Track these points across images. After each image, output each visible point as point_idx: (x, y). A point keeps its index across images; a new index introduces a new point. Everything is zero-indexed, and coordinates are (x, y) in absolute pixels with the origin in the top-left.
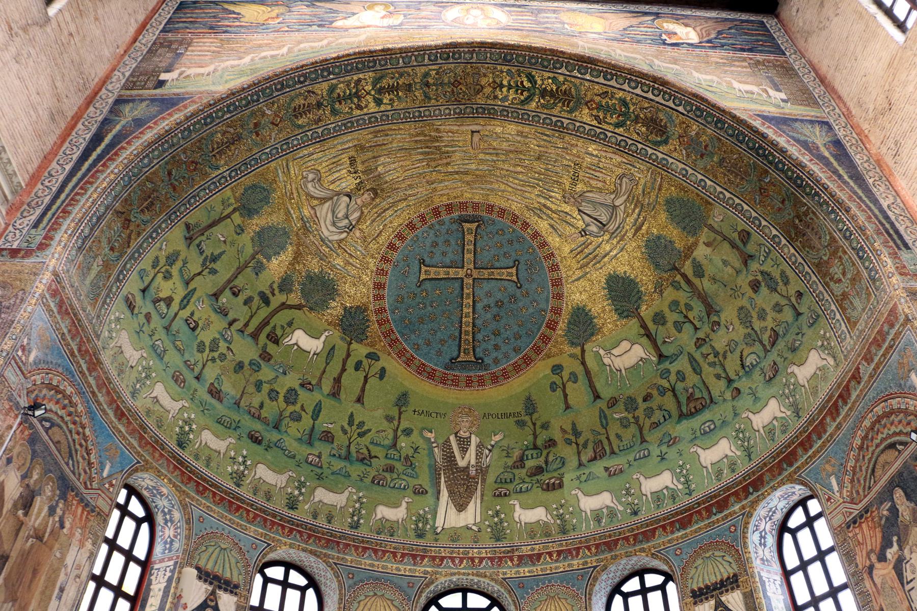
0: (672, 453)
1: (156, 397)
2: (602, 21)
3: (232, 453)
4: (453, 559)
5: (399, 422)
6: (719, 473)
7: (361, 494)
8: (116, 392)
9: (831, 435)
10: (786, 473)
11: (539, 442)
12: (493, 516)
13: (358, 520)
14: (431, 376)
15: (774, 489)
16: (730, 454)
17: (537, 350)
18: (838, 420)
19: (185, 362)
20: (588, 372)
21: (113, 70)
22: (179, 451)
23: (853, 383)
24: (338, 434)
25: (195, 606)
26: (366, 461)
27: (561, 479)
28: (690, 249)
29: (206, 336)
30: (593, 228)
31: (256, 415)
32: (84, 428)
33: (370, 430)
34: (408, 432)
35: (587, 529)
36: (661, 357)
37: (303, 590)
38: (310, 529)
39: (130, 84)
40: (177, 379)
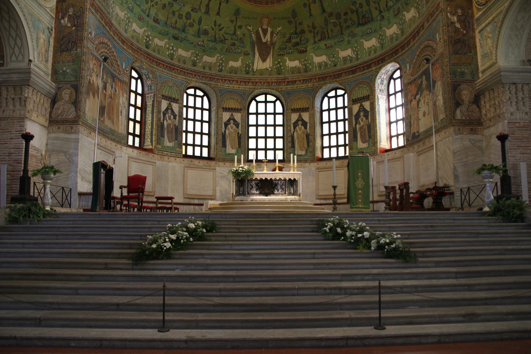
1: (134, 30)
3: (168, 46)
4: (261, 83)
5: (236, 23)
7: (222, 57)
8: (120, 33)
9: (411, 47)
10: (394, 58)
11: (298, 31)
12: (277, 64)
13: (222, 68)
15: (388, 63)
16: (375, 45)
18: (415, 41)
19: (142, 10)
22: (147, 50)
23: (421, 28)
24: (210, 30)
25: (164, 109)
26: (223, 42)
27: (306, 48)
31: (175, 27)
32: (113, 53)
33: (223, 28)
34: (240, 27)
35: (315, 71)
37: (202, 97)
38: (203, 74)
40: (140, 19)
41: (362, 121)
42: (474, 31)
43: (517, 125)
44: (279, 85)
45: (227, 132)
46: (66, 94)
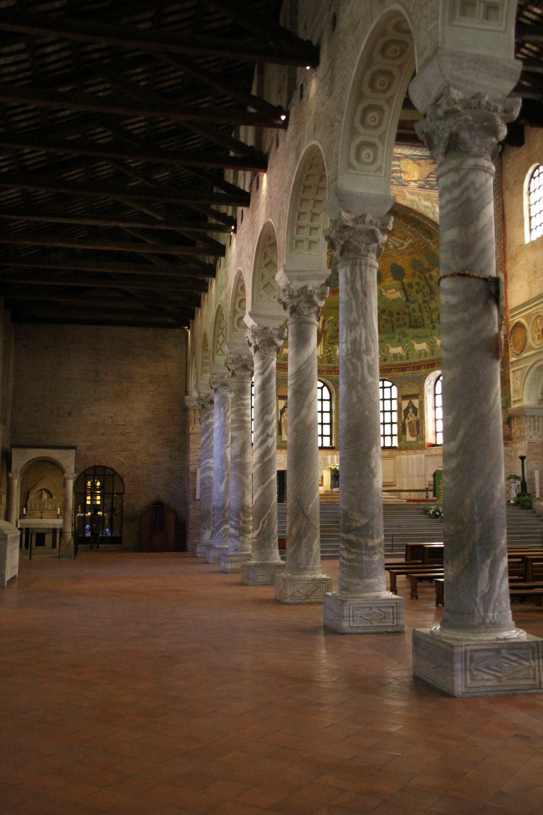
0: (404, 340)
2: (418, 168)
6: (420, 355)
12: (328, 352)
15: (438, 369)
16: (426, 349)
28: (429, 270)
30: (391, 247)
36: (407, 300)
41: (411, 416)
42: (509, 369)
43: (534, 444)
44: (330, 374)
45: (283, 420)
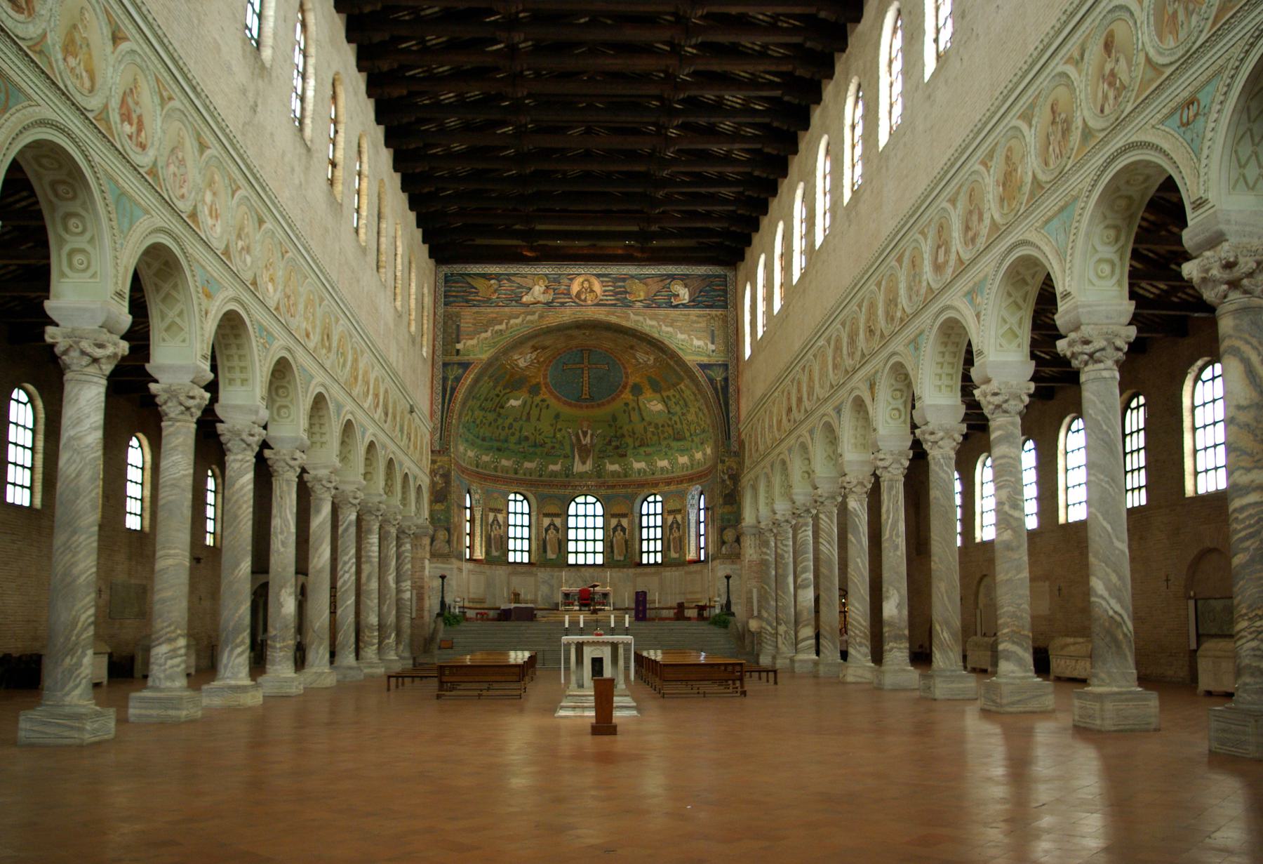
2: (645, 287)
14: (570, 405)
17: (619, 396)
20: (639, 408)
21: (434, 340)
28: (678, 384)
29: (478, 422)
34: (560, 430)
35: (635, 477)
39: (445, 352)
40: (473, 444)
46: (442, 535)
